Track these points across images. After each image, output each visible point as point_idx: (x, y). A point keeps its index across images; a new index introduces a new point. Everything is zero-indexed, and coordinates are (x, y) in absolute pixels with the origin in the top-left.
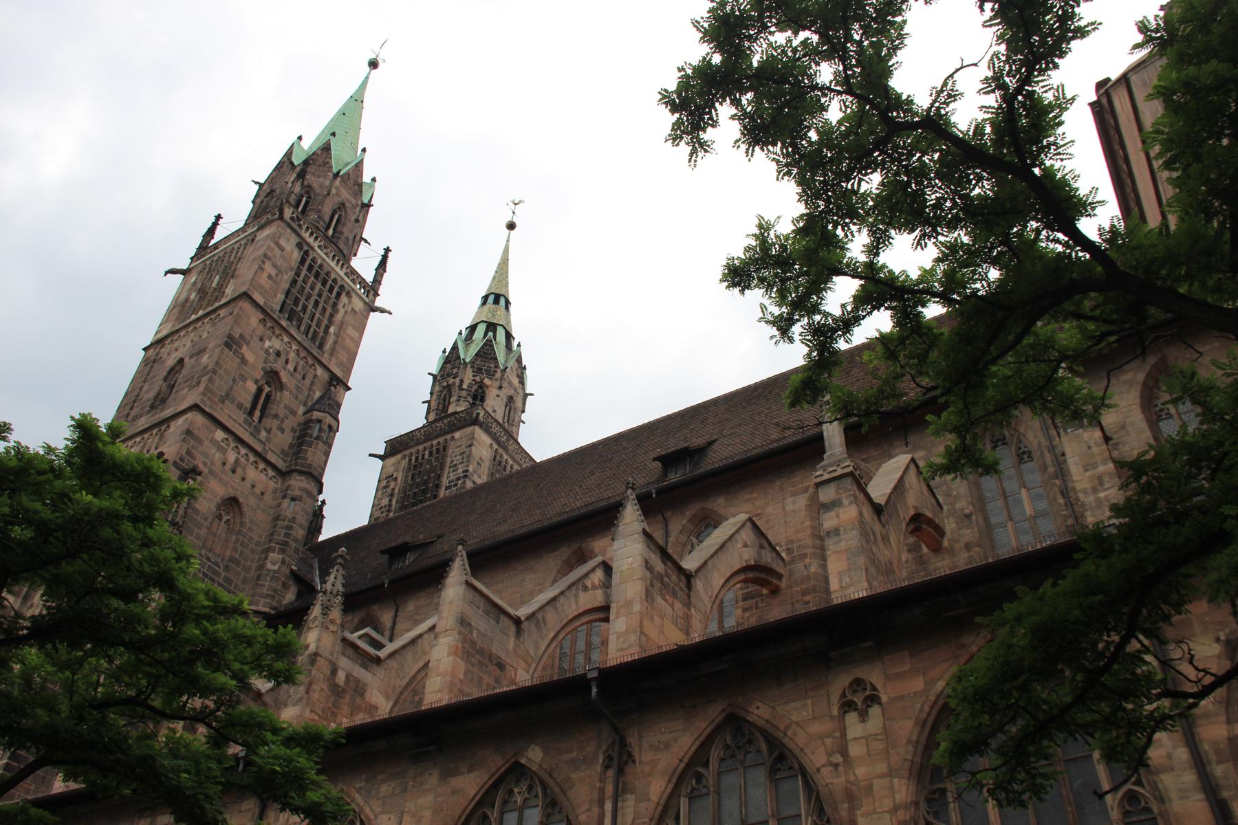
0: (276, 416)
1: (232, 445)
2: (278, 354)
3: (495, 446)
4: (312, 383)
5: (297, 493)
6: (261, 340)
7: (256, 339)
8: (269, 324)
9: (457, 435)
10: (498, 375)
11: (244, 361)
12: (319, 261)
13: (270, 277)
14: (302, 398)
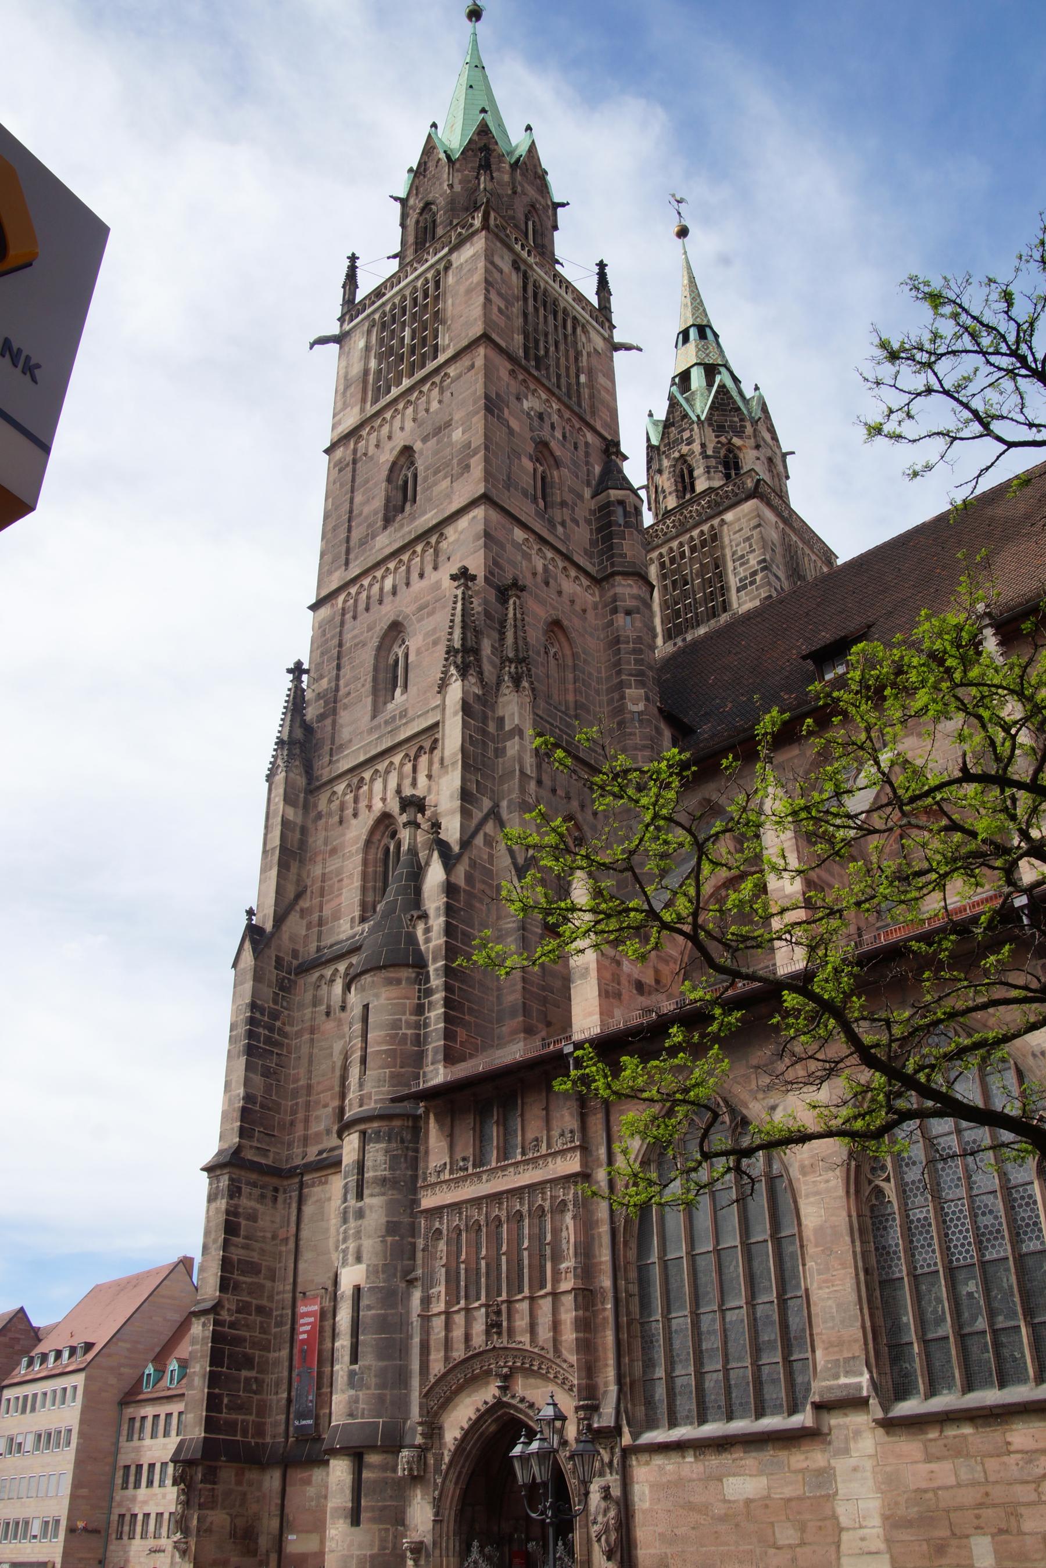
0: (563, 504)
1: (536, 547)
2: (541, 416)
3: (781, 526)
4: (587, 454)
5: (630, 603)
6: (518, 399)
7: (512, 399)
8: (521, 377)
9: (729, 516)
10: (749, 430)
11: (511, 432)
12: (542, 285)
13: (500, 310)
14: (583, 475)
